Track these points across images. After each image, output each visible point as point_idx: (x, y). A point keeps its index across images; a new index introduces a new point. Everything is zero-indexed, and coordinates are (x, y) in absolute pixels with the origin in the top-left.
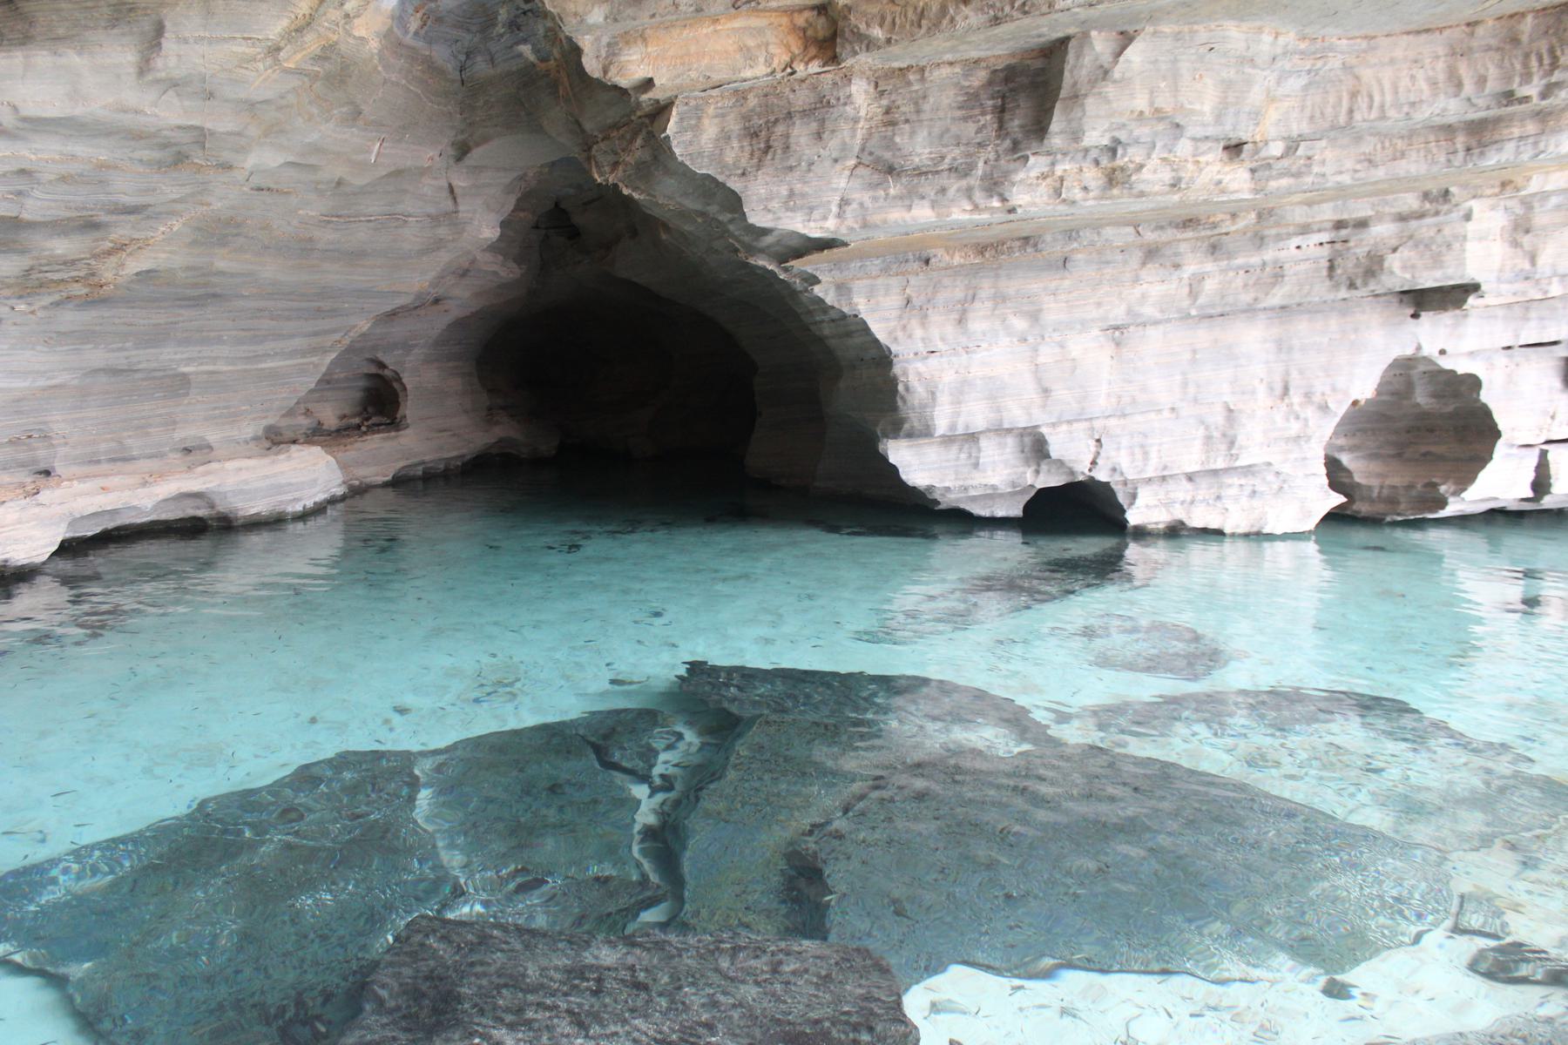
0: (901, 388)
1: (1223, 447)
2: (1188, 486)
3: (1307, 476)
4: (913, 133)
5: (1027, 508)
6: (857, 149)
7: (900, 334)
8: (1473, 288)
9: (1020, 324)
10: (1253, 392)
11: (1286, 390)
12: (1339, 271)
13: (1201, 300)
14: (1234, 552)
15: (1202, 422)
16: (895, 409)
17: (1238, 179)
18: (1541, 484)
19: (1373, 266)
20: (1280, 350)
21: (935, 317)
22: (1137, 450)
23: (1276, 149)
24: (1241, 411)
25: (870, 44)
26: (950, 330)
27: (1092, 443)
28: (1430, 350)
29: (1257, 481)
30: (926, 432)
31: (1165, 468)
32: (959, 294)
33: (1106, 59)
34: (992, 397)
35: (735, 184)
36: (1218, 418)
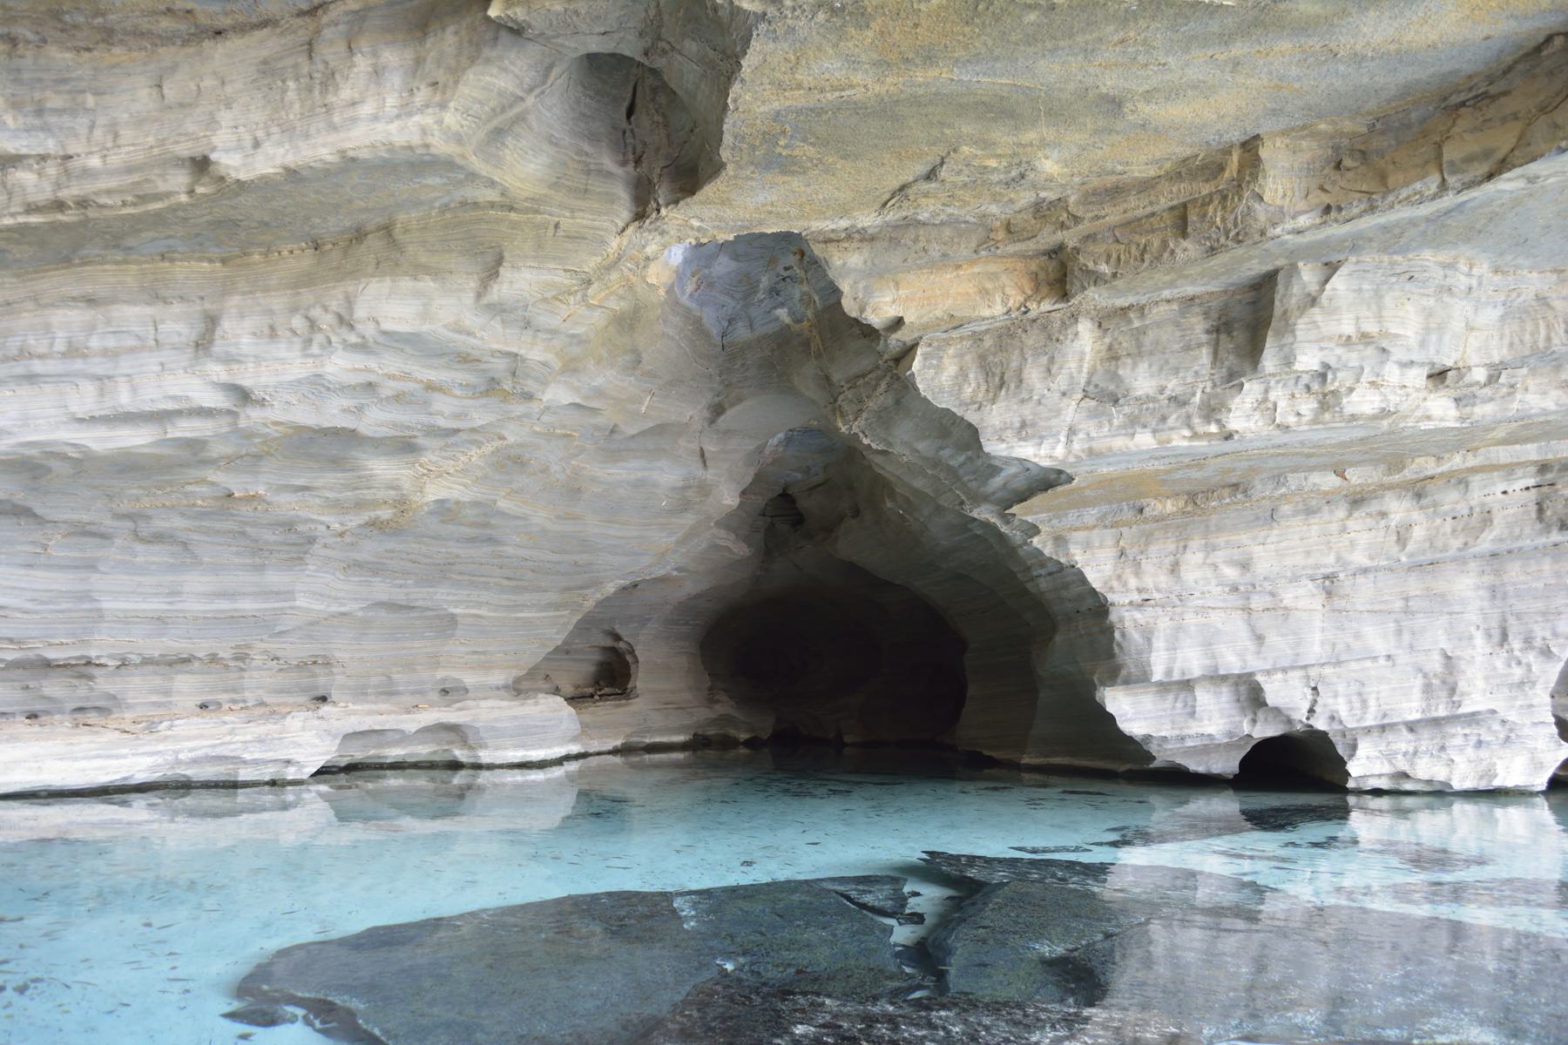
0: (1117, 635)
1: (1444, 694)
2: (1410, 736)
3: (1535, 724)
4: (1135, 365)
5: (1243, 763)
6: (1083, 381)
7: (1115, 584)
9: (1231, 573)
10: (1471, 638)
11: (1504, 636)
12: (1549, 513)
13: (1410, 547)
15: (1420, 670)
16: (1111, 655)
17: (1441, 409)
20: (1494, 597)
21: (1147, 566)
22: (1354, 699)
23: (1480, 375)
24: (1459, 658)
25: (1097, 279)
26: (1164, 580)
27: (1309, 691)
29: (1482, 731)
31: (1385, 716)
32: (1172, 547)
33: (1313, 288)
34: (1207, 644)
35: (971, 417)
36: (1435, 664)
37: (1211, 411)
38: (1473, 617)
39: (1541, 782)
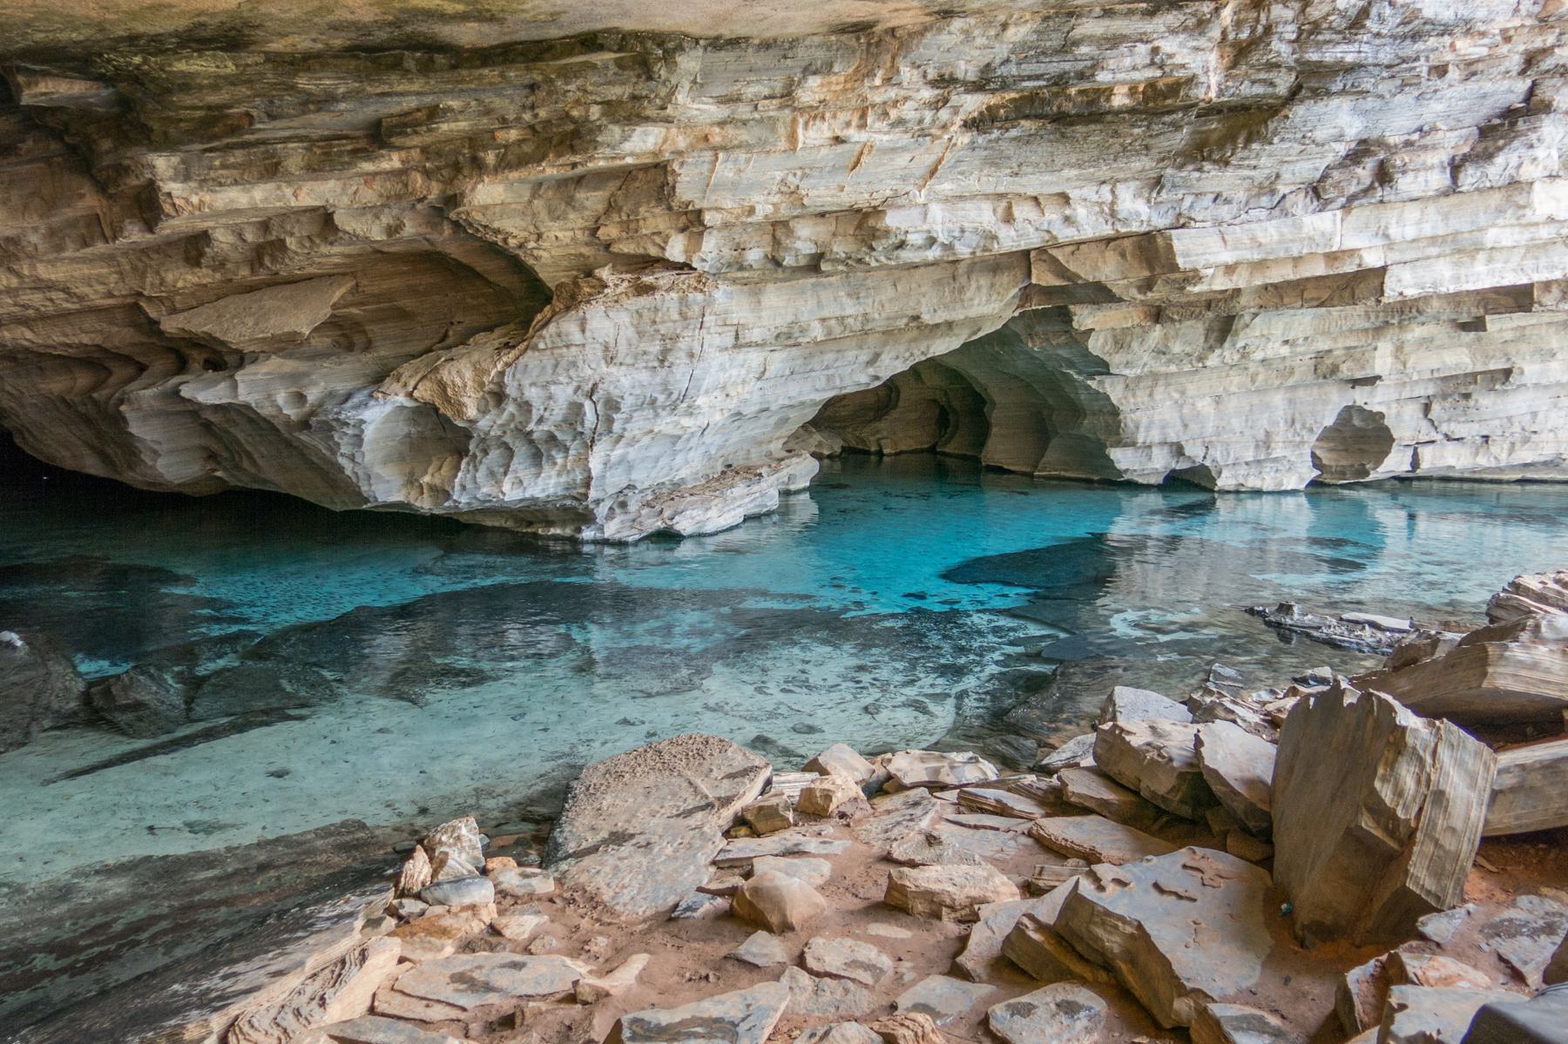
8: (1379, 378)
9: (1176, 396)
11: (1293, 422)
14: (1267, 501)
18: (1415, 463)
19: (1334, 369)
21: (1139, 393)
26: (1146, 399)
28: (1360, 403)
30: (1134, 444)
34: (1163, 428)
35: (1106, 358)
36: (1261, 436)
37: (1200, 359)
38: (1281, 413)
39: (1302, 487)
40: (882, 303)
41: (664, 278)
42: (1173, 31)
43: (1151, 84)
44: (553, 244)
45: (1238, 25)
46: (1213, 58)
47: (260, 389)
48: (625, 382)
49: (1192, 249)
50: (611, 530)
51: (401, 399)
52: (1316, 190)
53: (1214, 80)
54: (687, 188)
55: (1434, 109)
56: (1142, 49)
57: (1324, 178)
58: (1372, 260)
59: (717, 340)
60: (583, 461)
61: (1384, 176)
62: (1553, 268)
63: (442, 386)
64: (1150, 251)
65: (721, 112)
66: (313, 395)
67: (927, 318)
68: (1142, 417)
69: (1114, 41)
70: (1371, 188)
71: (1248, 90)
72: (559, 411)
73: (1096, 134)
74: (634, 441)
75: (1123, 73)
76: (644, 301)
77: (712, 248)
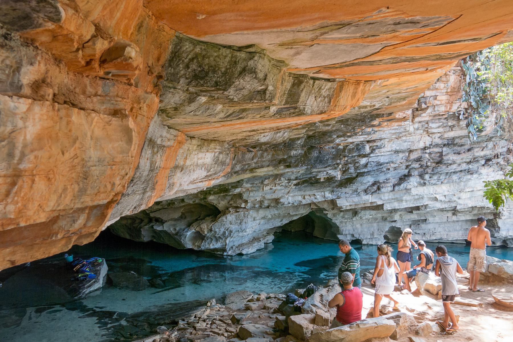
19: (386, 219)
28: (394, 226)
30: (342, 234)
37: (352, 219)
40: (282, 212)
41: (241, 210)
42: (331, 170)
43: (328, 177)
44: (221, 204)
45: (343, 168)
46: (339, 173)
47: (167, 227)
48: (233, 228)
49: (341, 203)
50: (230, 253)
51: (194, 230)
52: (366, 191)
53: (339, 176)
54: (245, 197)
55: (388, 176)
56: (325, 172)
57: (367, 189)
58: (380, 203)
59: (250, 220)
60: (225, 241)
61: (379, 189)
62: (420, 203)
63: (201, 228)
64: (333, 203)
65: (251, 186)
66: (177, 229)
67: (291, 214)
68: (344, 229)
69: (320, 172)
70: (376, 191)
71: (346, 177)
72: (221, 233)
73: (319, 185)
74: (235, 237)
75: (322, 176)
76: (237, 214)
77: (249, 205)
